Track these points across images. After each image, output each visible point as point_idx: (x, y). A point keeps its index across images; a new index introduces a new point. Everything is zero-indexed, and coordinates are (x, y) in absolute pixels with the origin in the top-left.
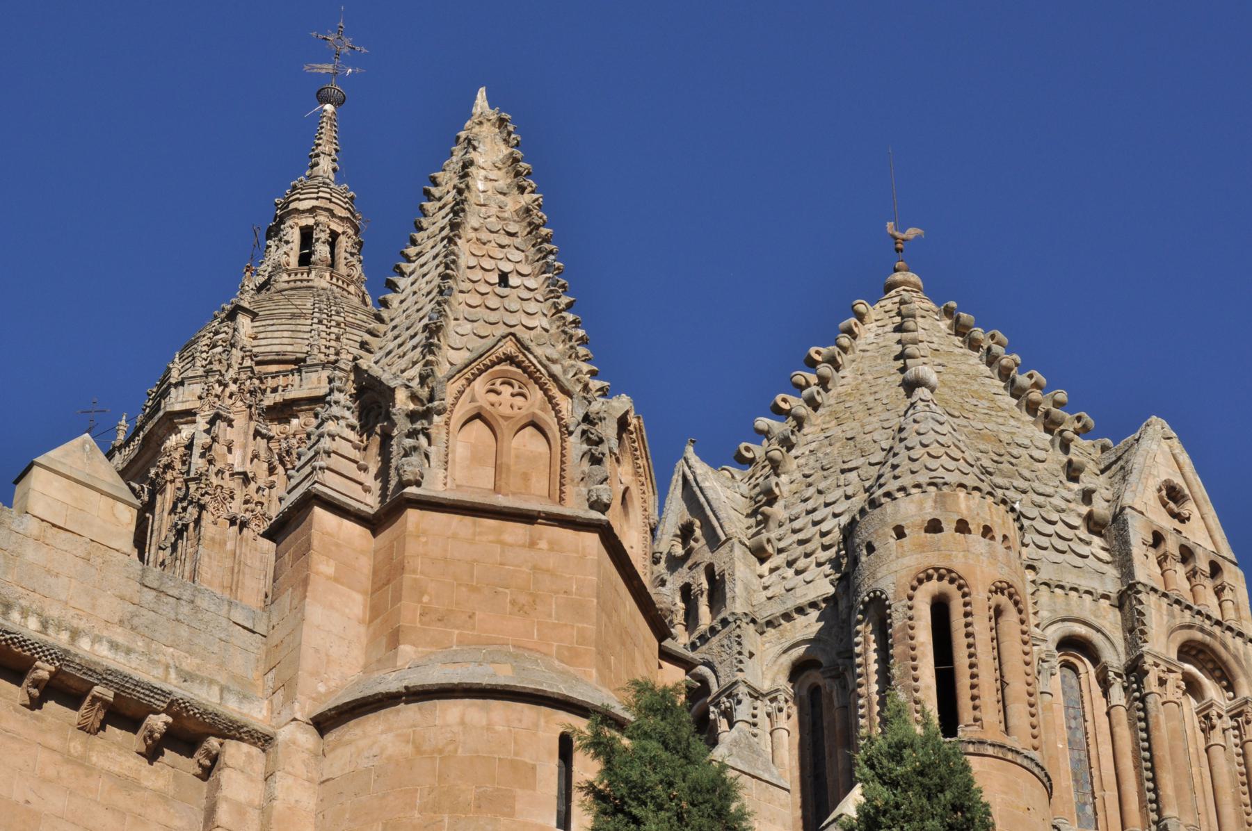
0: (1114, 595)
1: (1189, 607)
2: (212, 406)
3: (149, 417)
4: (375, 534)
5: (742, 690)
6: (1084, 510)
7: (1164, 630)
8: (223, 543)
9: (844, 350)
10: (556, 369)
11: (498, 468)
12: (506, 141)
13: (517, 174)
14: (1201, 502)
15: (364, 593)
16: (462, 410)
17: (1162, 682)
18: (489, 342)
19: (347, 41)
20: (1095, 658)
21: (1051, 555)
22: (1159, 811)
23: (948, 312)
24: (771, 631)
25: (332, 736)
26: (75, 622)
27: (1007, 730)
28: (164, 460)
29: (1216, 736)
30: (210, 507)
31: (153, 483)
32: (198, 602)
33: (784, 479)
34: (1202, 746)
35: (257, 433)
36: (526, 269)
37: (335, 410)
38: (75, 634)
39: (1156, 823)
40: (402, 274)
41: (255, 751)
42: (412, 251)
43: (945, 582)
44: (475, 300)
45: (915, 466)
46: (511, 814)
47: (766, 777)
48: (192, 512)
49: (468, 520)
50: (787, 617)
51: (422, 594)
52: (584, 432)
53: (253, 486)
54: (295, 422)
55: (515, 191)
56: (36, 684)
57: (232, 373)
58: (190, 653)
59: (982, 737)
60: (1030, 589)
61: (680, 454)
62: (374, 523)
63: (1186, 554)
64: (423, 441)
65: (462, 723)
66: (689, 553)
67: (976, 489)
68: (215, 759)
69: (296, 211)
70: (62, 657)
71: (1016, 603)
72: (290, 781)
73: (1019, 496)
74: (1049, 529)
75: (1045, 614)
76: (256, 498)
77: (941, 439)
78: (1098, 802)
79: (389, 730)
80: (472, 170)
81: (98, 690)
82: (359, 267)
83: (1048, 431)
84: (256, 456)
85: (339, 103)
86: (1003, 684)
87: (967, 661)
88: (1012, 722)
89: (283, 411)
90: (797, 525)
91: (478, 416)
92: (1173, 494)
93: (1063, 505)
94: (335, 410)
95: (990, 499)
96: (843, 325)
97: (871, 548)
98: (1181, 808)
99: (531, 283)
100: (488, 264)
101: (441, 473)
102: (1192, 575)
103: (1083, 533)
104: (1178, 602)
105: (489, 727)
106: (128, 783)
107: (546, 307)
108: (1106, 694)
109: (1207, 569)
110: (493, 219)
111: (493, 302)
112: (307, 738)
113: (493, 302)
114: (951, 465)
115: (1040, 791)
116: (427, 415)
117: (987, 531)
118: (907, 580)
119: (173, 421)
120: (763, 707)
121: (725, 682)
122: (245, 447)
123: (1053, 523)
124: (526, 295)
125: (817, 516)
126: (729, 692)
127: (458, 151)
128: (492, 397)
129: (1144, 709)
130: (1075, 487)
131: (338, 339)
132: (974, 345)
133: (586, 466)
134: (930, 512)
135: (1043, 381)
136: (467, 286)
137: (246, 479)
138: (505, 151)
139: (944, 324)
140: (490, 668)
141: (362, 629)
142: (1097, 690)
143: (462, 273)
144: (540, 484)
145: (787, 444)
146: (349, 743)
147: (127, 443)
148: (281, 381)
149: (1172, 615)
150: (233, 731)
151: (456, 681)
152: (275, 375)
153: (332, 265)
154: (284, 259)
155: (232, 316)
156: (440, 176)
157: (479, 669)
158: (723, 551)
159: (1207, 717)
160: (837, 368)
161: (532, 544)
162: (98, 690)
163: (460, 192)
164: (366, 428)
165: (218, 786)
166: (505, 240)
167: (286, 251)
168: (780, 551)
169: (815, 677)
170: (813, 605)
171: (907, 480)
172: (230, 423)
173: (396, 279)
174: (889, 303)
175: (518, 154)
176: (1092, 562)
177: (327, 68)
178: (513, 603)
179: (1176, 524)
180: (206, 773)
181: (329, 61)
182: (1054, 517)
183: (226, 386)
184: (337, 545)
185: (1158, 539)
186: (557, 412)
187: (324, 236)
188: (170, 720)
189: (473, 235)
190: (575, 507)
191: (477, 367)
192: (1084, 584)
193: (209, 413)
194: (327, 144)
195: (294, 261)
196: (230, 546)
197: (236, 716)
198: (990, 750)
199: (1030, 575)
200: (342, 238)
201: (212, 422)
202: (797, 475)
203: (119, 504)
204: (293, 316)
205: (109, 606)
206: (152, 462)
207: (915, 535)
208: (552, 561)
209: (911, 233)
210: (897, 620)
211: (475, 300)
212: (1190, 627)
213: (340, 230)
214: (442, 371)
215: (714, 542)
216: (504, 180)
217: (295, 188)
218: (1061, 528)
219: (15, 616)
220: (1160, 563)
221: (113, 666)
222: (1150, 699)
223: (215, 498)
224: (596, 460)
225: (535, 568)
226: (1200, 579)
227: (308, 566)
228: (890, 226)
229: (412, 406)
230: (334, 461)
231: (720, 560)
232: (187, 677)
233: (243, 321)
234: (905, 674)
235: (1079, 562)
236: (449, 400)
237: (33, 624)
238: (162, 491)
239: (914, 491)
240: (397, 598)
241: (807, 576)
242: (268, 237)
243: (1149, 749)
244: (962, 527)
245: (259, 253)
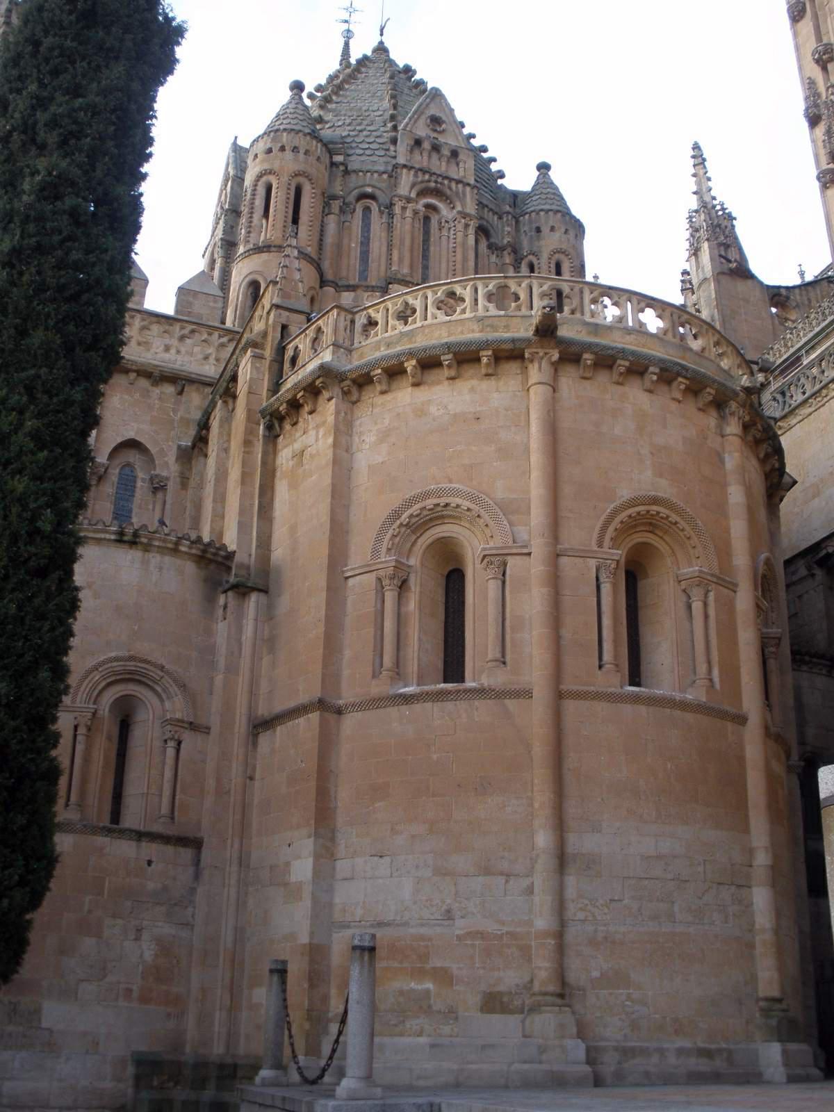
29: (445, 232)
63: (436, 148)
134: (269, 145)
179: (435, 135)
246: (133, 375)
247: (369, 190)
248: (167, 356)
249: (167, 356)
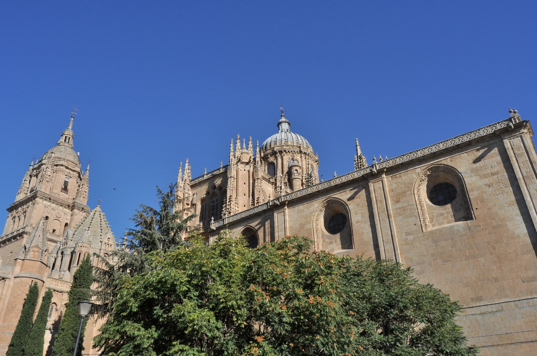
16: (32, 250)
28: (41, 169)
57: (50, 162)
74: (96, 242)
112: (13, 278)
119: (42, 164)
126: (65, 254)
133: (41, 256)
137: (50, 176)
147: (37, 164)
150: (7, 278)
153: (68, 143)
167: (62, 139)
177: (73, 113)
191: (34, 247)
192: (97, 248)
195: (64, 141)
204: (61, 152)
208: (36, 264)
210: (76, 254)
244: (84, 247)
247: (95, 252)
248: (61, 287)
249: (61, 287)
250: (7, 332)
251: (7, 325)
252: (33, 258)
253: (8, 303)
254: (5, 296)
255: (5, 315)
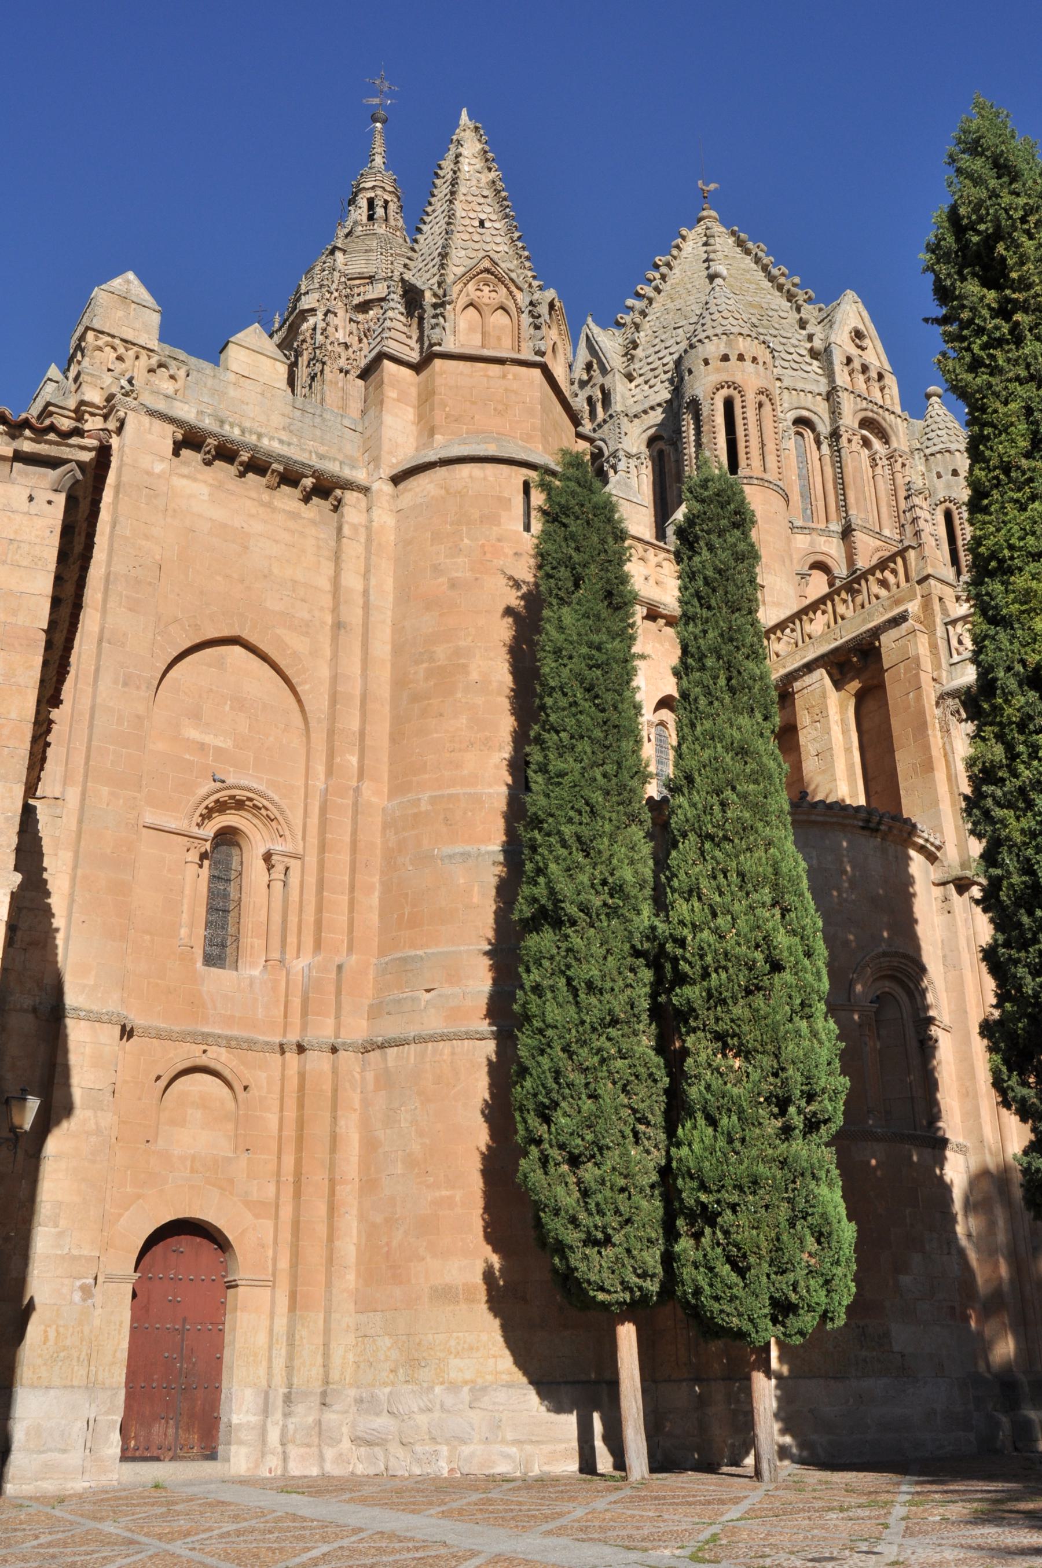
0: (824, 394)
1: (865, 399)
2: (325, 305)
3: (291, 313)
4: (418, 373)
5: (621, 454)
6: (809, 345)
7: (851, 412)
8: (337, 383)
9: (675, 258)
10: (513, 275)
11: (483, 334)
12: (480, 141)
13: (487, 160)
14: (873, 338)
15: (414, 407)
16: (462, 302)
17: (850, 441)
18: (475, 261)
19: (387, 84)
20: (813, 429)
21: (790, 372)
22: (846, 512)
23: (733, 233)
24: (636, 420)
25: (401, 486)
26: (259, 430)
27: (765, 470)
28: (301, 338)
29: (879, 470)
30: (328, 363)
31: (296, 351)
32: (325, 415)
33: (642, 334)
34: (871, 475)
35: (351, 320)
36: (494, 217)
37: (392, 304)
38: (260, 436)
39: (845, 518)
40: (425, 223)
41: (361, 496)
42: (429, 209)
43: (731, 389)
44: (466, 237)
45: (714, 324)
46: (499, 524)
47: (635, 500)
48: (319, 366)
49: (468, 364)
50: (645, 412)
51: (446, 406)
52: (530, 311)
53: (351, 350)
54: (371, 312)
55: (486, 171)
56: (241, 464)
57: (334, 286)
58: (323, 444)
59: (751, 474)
60: (778, 391)
61: (584, 322)
62: (417, 368)
63: (865, 369)
64: (441, 320)
65: (471, 477)
66: (590, 378)
67: (749, 335)
68: (339, 501)
69: (364, 188)
70: (254, 449)
71: (770, 400)
72: (380, 511)
73: (773, 339)
74: (789, 357)
75: (786, 405)
76: (353, 357)
77: (729, 308)
78: (814, 508)
79: (431, 482)
80: (461, 159)
81: (274, 466)
82: (401, 220)
83: (789, 301)
84: (351, 333)
85: (384, 122)
86: (763, 445)
87: (743, 433)
88: (768, 466)
89: (364, 307)
90: (650, 360)
91: (471, 304)
92: (858, 335)
93: (797, 343)
94: (392, 304)
95: (756, 341)
96: (674, 243)
97: (690, 372)
98: (858, 509)
99: (497, 225)
100: (472, 215)
101: (452, 338)
102: (868, 380)
103: (808, 359)
104: (859, 396)
105: (485, 479)
106: (294, 516)
107: (506, 239)
108: (819, 448)
109: (876, 376)
110: (474, 188)
111: (476, 237)
112: (388, 488)
113: (476, 237)
114: (735, 322)
115: (783, 503)
116: (443, 305)
117: (754, 360)
118: (710, 389)
119: (304, 315)
120: (633, 462)
121: (612, 449)
122: (345, 328)
123: (791, 354)
124: (495, 232)
125: (660, 355)
126: (614, 454)
127: (452, 147)
128: (478, 293)
129: (840, 456)
130: (804, 332)
131: (392, 263)
132: (748, 252)
133: (532, 330)
134: (723, 350)
135: (787, 272)
136: (461, 228)
137: (347, 346)
138: (479, 146)
139: (731, 240)
140: (484, 446)
141: (414, 428)
142: (814, 446)
143: (458, 221)
144: (507, 342)
145: (644, 314)
146: (410, 490)
147: (280, 329)
148: (362, 289)
149: (856, 404)
150: (348, 485)
151: (466, 454)
152: (358, 286)
153: (386, 220)
154: (359, 218)
155: (332, 252)
156: (443, 163)
157: (478, 447)
158: (609, 376)
159: (874, 459)
160: (671, 269)
161: (504, 376)
162: (274, 466)
163: (455, 172)
164: (409, 314)
165: (342, 516)
166: (482, 200)
167: (359, 213)
168: (641, 375)
169: (660, 445)
170: (659, 405)
171: (710, 332)
172: (336, 315)
173: (421, 226)
174: (700, 229)
175: (487, 148)
176: (812, 375)
177: (376, 101)
178: (495, 409)
179: (859, 351)
180: (336, 509)
181: (377, 97)
182: (792, 350)
183: (332, 293)
184: (398, 381)
185: (849, 360)
186: (515, 300)
187: (381, 203)
188: (314, 481)
189: (463, 198)
190: (527, 355)
191: (470, 275)
192: (808, 388)
193: (323, 309)
194: (379, 147)
195: (364, 218)
196: (340, 384)
197: (349, 477)
198: (756, 482)
199: (778, 384)
200: (391, 204)
201: (326, 315)
202: (650, 332)
203: (278, 363)
204: (366, 251)
205: (277, 420)
206: (295, 339)
207: (715, 363)
209: (712, 186)
210: (705, 411)
211: (466, 237)
212: (866, 410)
213: (389, 199)
214: (450, 279)
215: (604, 371)
216: (479, 164)
217: (362, 175)
218: (795, 357)
219: (227, 427)
220: (850, 375)
221: (282, 453)
222: (843, 451)
223: (330, 358)
224: (537, 327)
225: (506, 390)
226: (872, 382)
227: (382, 394)
228: (700, 182)
229: (434, 300)
230: (393, 334)
231: (607, 381)
232: (321, 457)
233: (339, 255)
234: (709, 441)
235: (805, 375)
236: (454, 296)
237: (237, 431)
238: (301, 355)
239: (714, 338)
240: (432, 410)
241: (655, 389)
242: (350, 205)
243: (842, 478)
244: (741, 358)
245: (344, 215)
246: (662, 622)
247: (805, 413)
250: (448, 850)
251: (433, 800)
252: (483, 346)
253: (397, 650)
254: (366, 607)
255: (396, 737)
